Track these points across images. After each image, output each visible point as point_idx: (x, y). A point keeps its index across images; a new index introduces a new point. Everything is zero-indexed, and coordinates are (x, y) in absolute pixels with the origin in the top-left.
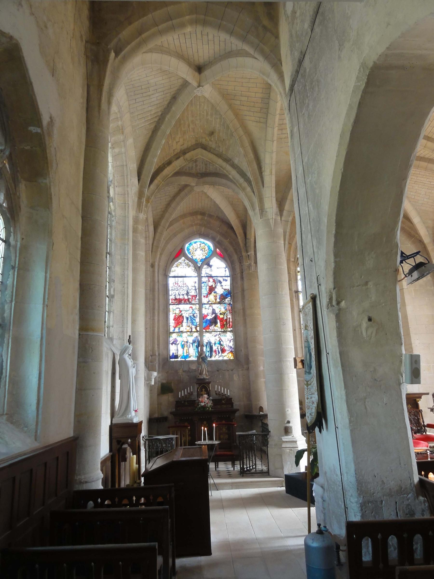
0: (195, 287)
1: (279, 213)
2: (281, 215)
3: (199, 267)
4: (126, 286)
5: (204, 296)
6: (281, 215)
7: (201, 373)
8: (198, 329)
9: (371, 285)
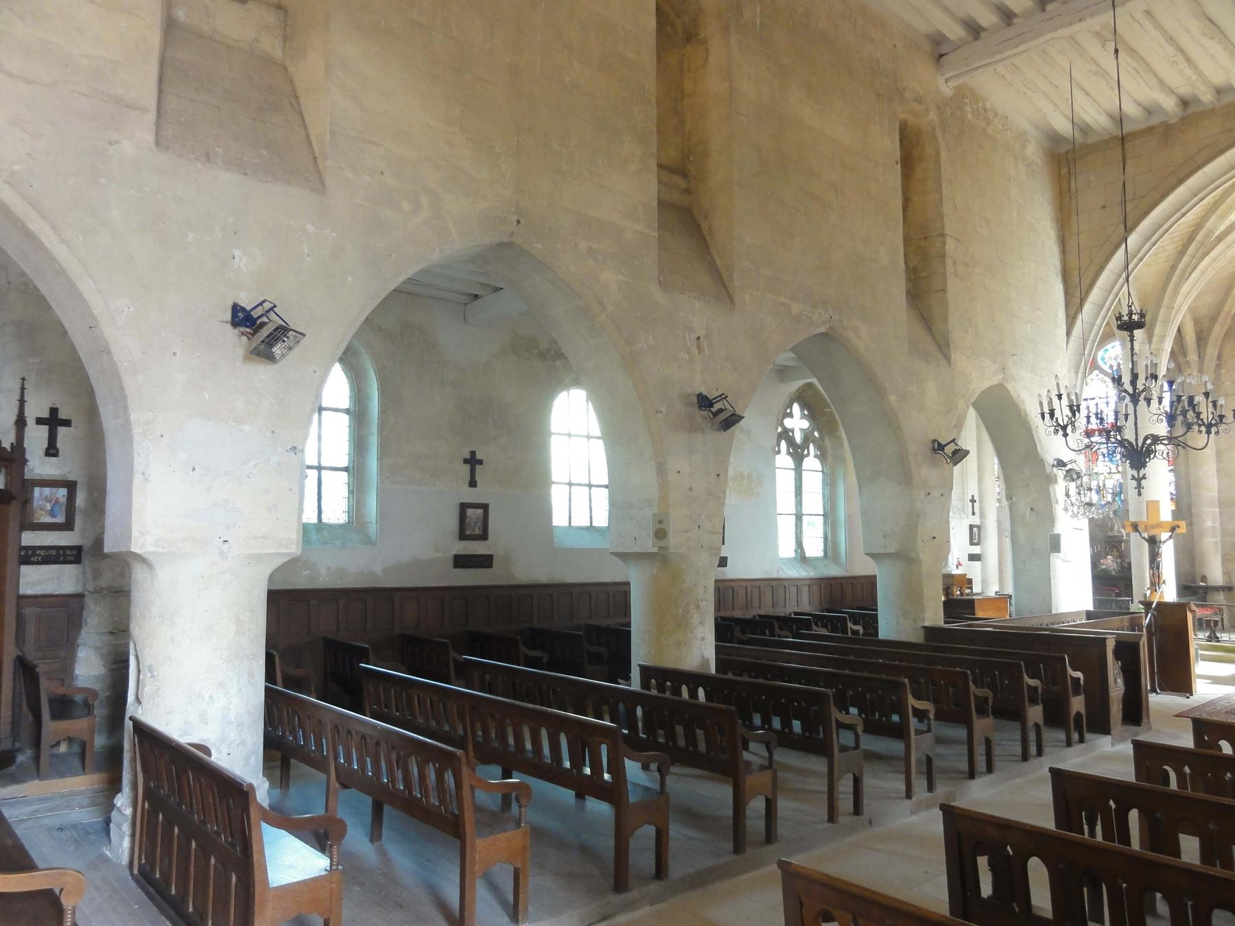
2: (1150, 342)
6: (1150, 342)
7: (1112, 530)
8: (1120, 469)
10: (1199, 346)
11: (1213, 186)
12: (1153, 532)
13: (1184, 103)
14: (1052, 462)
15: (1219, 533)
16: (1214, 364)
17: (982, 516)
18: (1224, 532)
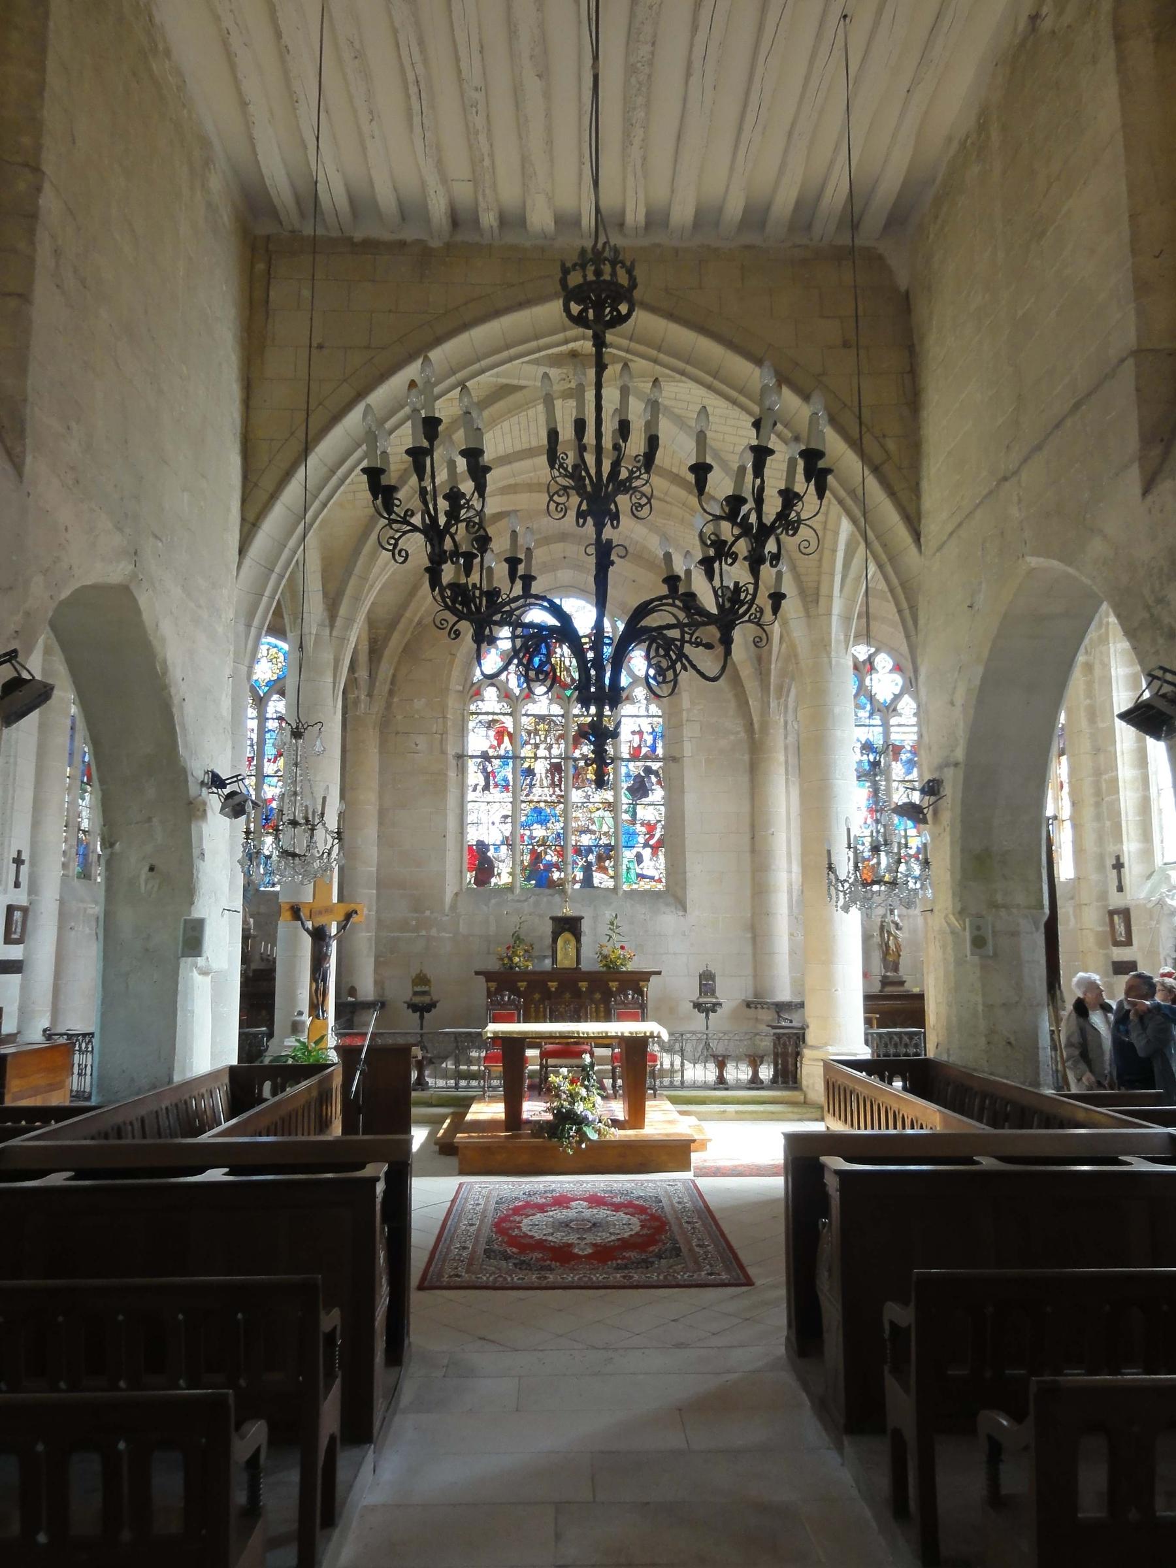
0: (252, 739)
1: (327, 622)
2: (332, 626)
3: (261, 699)
4: (12, 760)
5: (269, 760)
6: (332, 626)
9: (154, 820)
10: (371, 660)
11: (477, 366)
12: (321, 921)
13: (455, 221)
14: (200, 775)
15: (373, 925)
16: (387, 687)
17: (33, 890)
18: (379, 922)
